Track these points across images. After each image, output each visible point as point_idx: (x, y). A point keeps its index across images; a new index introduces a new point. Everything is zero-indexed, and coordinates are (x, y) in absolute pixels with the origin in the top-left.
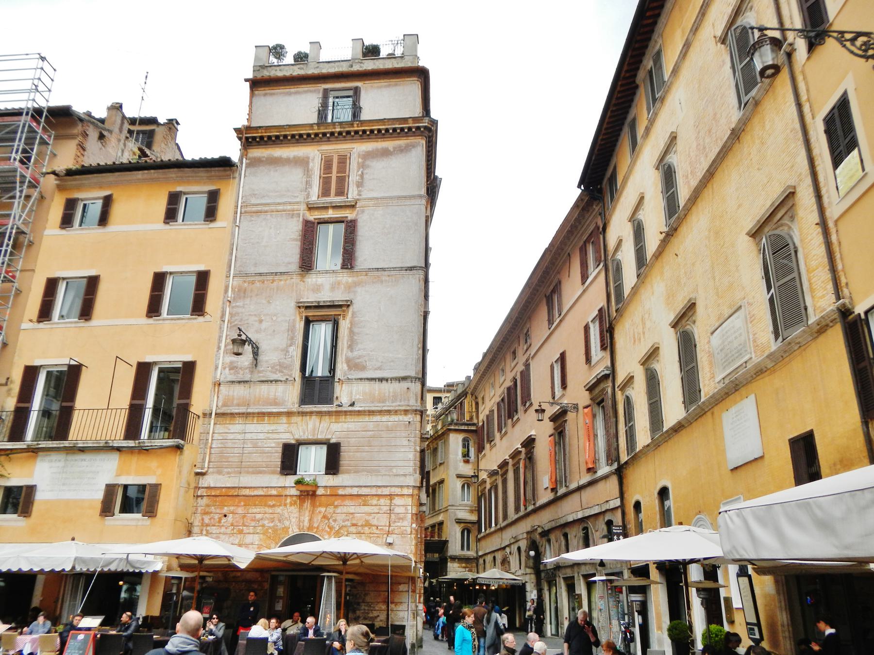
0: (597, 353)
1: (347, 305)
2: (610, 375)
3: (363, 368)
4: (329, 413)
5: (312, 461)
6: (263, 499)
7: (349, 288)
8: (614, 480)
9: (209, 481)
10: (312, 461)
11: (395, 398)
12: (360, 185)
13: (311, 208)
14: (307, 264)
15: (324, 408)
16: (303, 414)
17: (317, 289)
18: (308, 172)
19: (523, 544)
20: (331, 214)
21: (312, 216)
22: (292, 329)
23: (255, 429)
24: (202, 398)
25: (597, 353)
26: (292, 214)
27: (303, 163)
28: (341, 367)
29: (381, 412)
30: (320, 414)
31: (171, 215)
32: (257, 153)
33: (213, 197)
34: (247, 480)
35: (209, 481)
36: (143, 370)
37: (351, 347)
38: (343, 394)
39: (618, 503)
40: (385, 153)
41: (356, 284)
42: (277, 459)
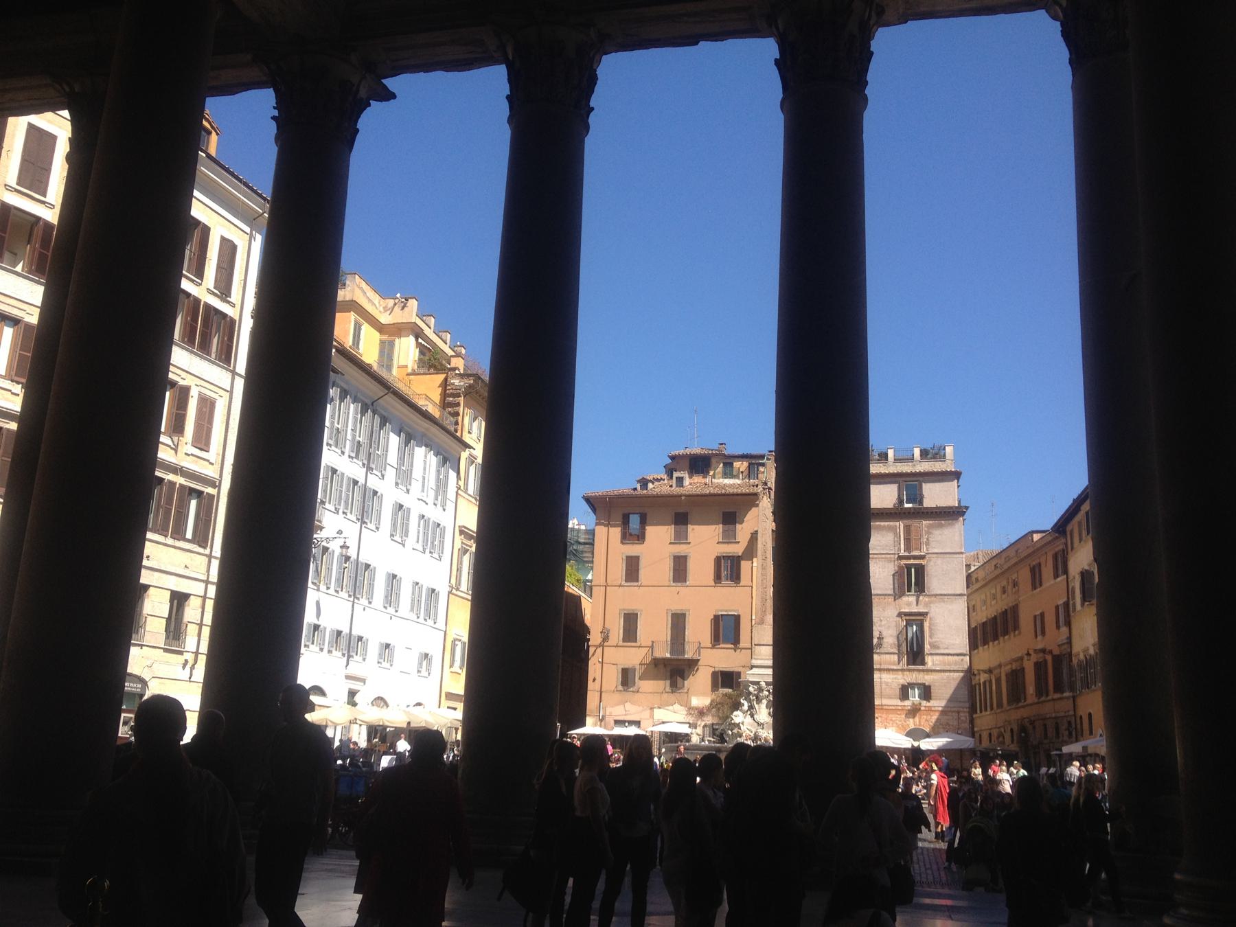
1: (927, 613)
3: (938, 648)
4: (923, 671)
6: (895, 710)
11: (956, 664)
12: (927, 544)
13: (900, 558)
15: (921, 667)
16: (909, 670)
17: (909, 604)
19: (1015, 728)
20: (912, 562)
26: (890, 561)
27: (893, 529)
28: (927, 647)
29: (950, 671)
30: (919, 671)
37: (931, 637)
38: (930, 661)
39: (1072, 713)
40: (941, 526)
41: (930, 602)
42: (898, 692)
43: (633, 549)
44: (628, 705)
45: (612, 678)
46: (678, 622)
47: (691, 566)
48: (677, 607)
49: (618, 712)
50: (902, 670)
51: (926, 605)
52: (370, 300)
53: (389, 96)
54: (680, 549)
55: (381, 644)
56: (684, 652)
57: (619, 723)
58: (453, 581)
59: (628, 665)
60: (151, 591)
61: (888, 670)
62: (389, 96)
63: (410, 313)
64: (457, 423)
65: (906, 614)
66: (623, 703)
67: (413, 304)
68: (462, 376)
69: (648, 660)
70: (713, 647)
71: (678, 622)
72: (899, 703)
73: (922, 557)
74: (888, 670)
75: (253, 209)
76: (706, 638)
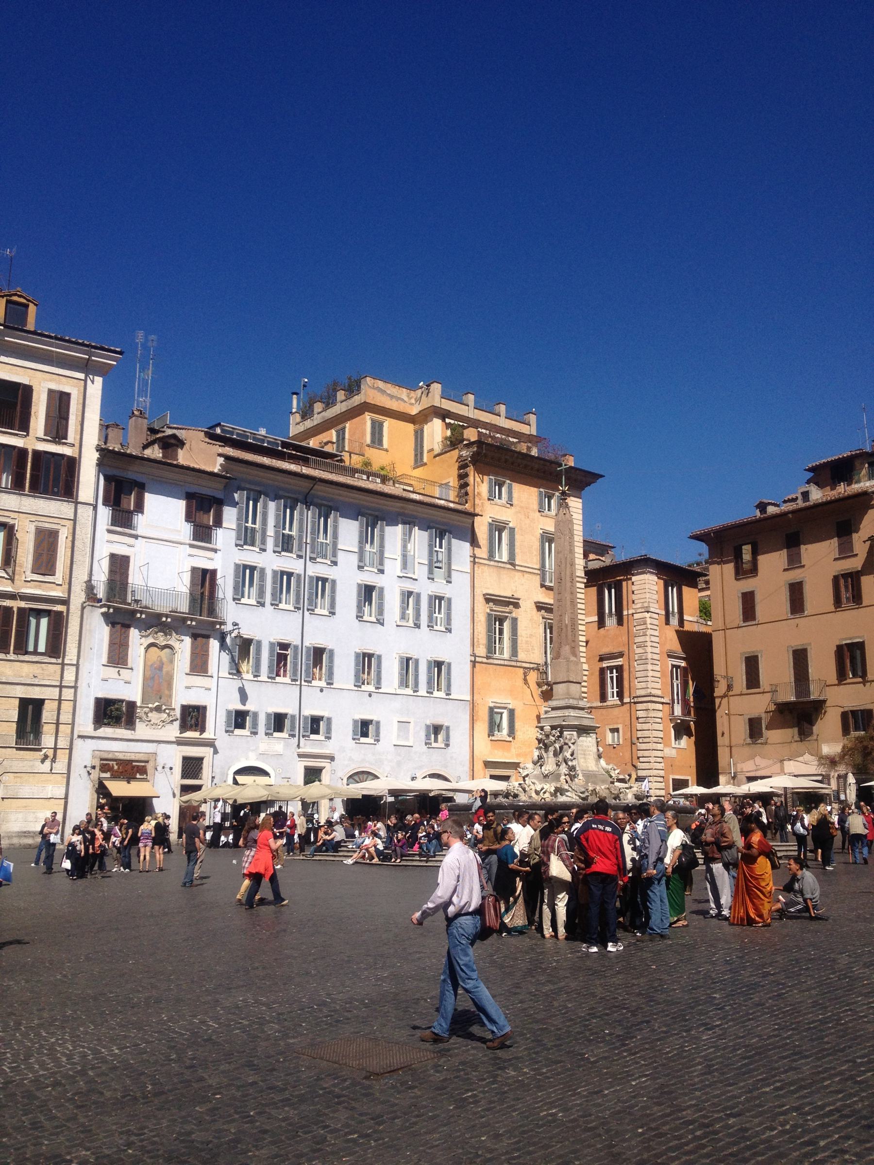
43: (747, 585)
44: (758, 759)
45: (741, 730)
46: (800, 657)
48: (798, 643)
49: (748, 767)
52: (392, 397)
54: (795, 575)
55: (355, 722)
56: (808, 693)
58: (481, 651)
59: (754, 714)
60: (46, 701)
63: (436, 396)
64: (467, 494)
66: (752, 757)
67: (436, 388)
68: (468, 446)
69: (773, 707)
70: (839, 684)
71: (800, 657)
75: (81, 358)
76: (831, 675)
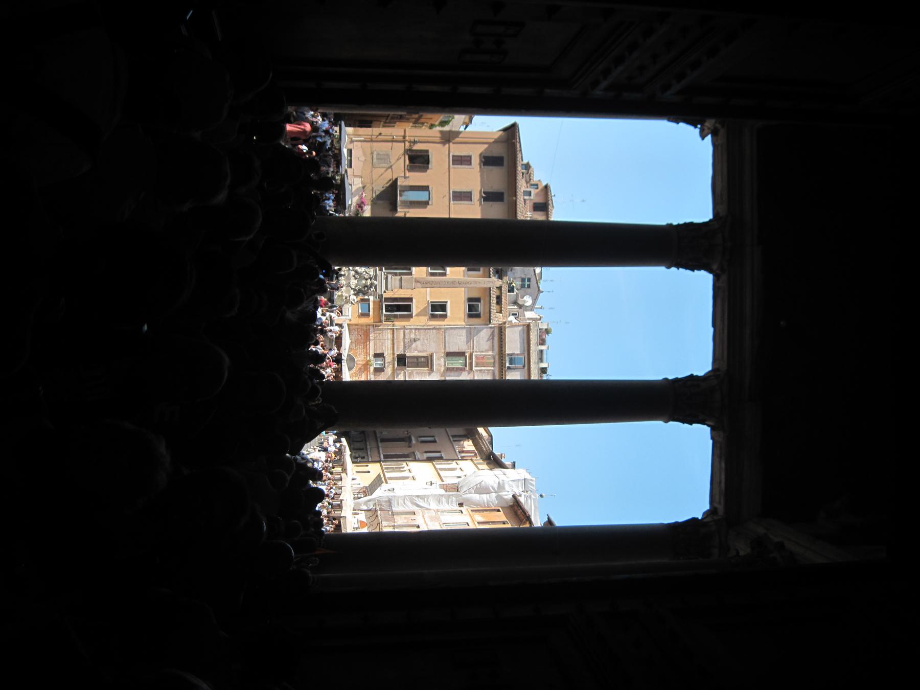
0: (426, 455)
2: (415, 460)
5: (378, 363)
7: (438, 370)
8: (378, 459)
9: (371, 329)
10: (378, 363)
14: (449, 354)
18: (487, 351)
21: (467, 355)
22: (424, 351)
23: (389, 343)
24: (398, 324)
25: (426, 455)
31: (470, 300)
32: (496, 331)
33: (478, 316)
34: (372, 343)
35: (371, 329)
36: (410, 299)
43: (476, 161)
47: (464, 204)
50: (393, 354)
51: (438, 370)
53: (703, 137)
57: (350, 152)
61: (393, 344)
62: (703, 137)
65: (432, 356)
66: (365, 155)
72: (372, 353)
73: (471, 369)
74: (393, 344)
